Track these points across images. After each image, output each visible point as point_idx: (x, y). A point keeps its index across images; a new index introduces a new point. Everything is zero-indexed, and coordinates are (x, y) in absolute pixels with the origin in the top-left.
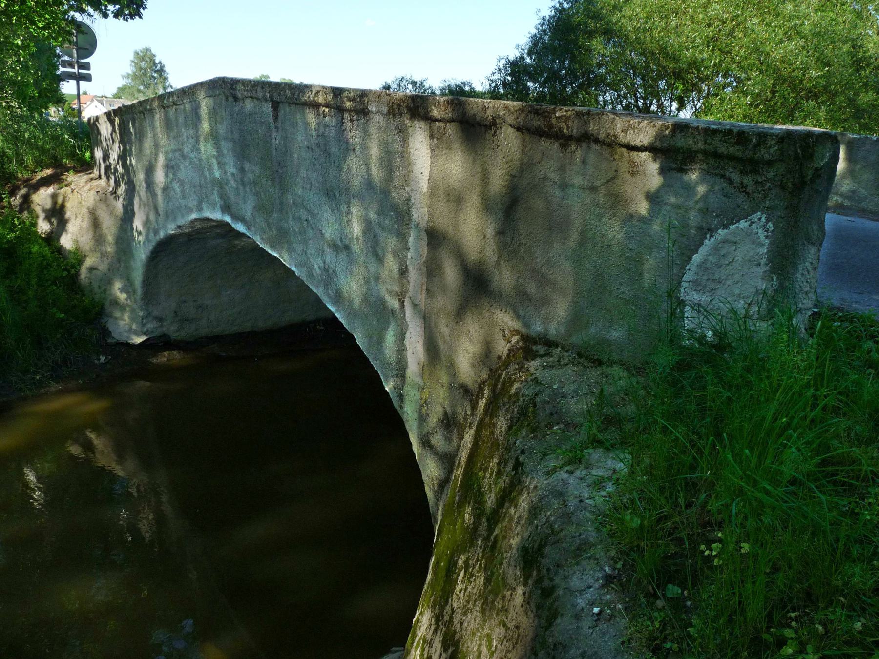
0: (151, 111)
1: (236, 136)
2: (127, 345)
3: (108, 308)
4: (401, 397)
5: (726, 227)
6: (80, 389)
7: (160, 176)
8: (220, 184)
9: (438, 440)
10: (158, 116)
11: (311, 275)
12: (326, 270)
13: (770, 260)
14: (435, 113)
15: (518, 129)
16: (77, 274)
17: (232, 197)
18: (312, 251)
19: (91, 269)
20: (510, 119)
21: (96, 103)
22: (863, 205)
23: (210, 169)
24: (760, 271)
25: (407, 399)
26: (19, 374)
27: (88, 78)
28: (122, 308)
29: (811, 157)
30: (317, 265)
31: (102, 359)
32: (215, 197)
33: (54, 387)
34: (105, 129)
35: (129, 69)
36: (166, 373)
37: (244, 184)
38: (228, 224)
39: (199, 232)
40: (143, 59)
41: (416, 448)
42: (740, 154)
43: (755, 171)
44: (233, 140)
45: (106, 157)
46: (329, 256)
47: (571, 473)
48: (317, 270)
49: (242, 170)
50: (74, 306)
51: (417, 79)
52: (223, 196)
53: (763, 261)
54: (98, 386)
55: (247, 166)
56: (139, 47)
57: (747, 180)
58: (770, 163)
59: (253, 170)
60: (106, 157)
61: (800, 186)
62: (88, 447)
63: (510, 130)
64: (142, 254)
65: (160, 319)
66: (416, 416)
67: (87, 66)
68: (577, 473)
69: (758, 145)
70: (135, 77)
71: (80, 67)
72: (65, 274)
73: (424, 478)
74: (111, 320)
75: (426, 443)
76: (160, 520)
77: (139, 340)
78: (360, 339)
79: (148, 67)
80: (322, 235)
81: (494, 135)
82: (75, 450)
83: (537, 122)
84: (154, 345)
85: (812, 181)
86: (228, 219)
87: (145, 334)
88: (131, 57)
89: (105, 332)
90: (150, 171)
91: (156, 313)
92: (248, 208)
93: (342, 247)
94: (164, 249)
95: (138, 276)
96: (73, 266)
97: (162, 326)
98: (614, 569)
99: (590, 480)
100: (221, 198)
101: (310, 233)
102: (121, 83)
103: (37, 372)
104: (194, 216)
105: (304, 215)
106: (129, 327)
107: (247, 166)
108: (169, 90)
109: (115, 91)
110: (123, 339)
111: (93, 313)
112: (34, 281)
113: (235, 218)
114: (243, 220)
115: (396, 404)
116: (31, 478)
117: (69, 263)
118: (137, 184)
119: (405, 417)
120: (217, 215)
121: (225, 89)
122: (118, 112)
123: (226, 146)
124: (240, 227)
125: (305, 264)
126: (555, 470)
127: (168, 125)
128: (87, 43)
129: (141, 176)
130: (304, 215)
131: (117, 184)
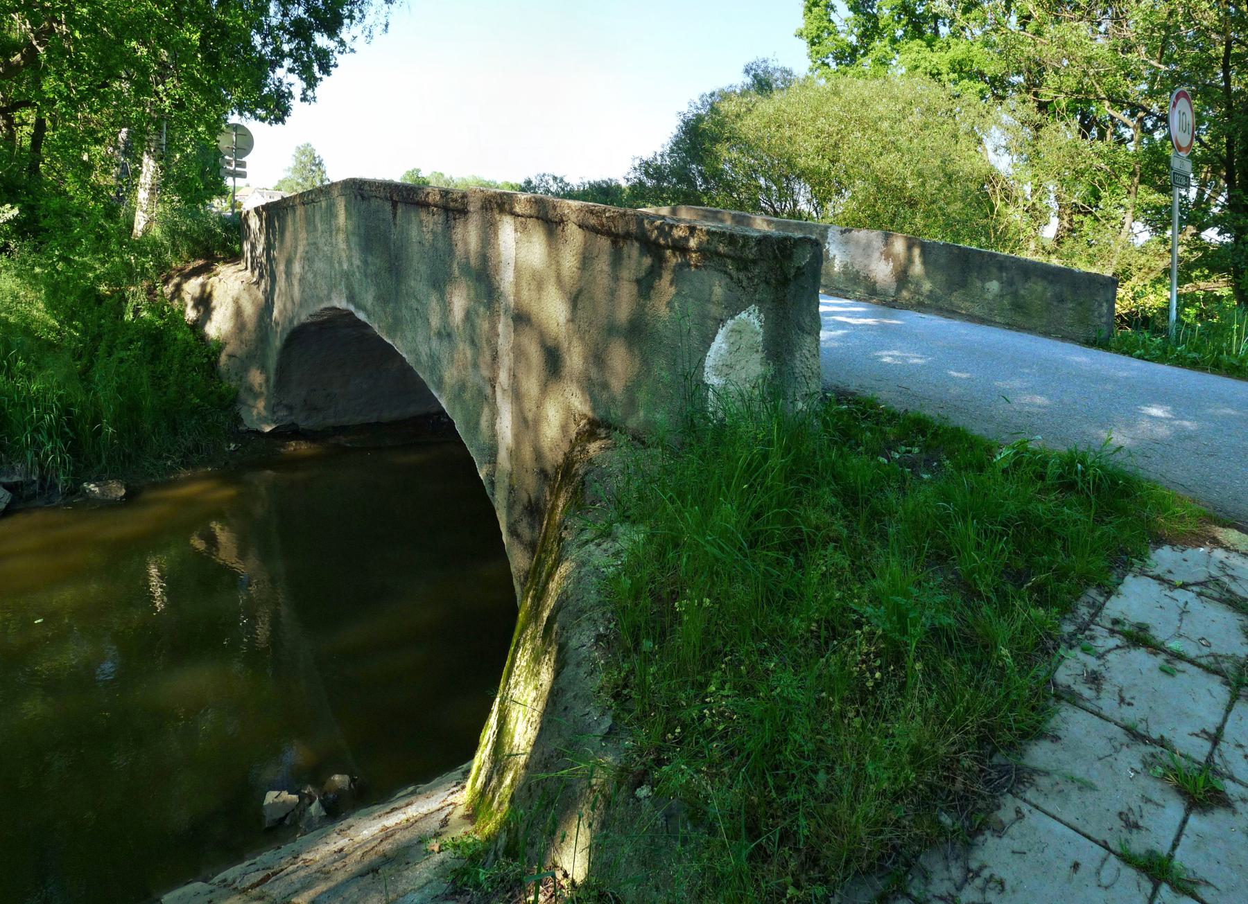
0: (293, 207)
1: (362, 231)
2: (259, 433)
3: (243, 395)
4: (492, 483)
5: (732, 317)
6: (208, 477)
7: (297, 268)
8: (347, 275)
9: (524, 530)
10: (300, 211)
11: (418, 361)
12: (431, 356)
13: (766, 348)
14: (518, 209)
15: (580, 226)
16: (217, 361)
17: (356, 286)
18: (420, 338)
19: (230, 356)
20: (573, 217)
21: (257, 194)
22: (940, 303)
23: (340, 263)
24: (758, 357)
25: (497, 485)
26: (152, 460)
27: (243, 175)
28: (257, 396)
29: (790, 257)
30: (424, 350)
31: (233, 446)
32: (343, 287)
33: (184, 473)
34: (254, 223)
35: (292, 163)
36: (294, 462)
37: (366, 276)
38: (352, 314)
39: (329, 321)
40: (303, 153)
41: (505, 538)
42: (731, 253)
43: (746, 269)
44: (359, 235)
45: (253, 248)
46: (435, 343)
47: (599, 545)
48: (424, 358)
49: (365, 262)
50: (211, 393)
51: (558, 175)
52: (350, 287)
53: (760, 349)
54: (229, 474)
55: (370, 259)
56: (301, 143)
57: (742, 275)
58: (754, 262)
59: (376, 262)
60: (253, 248)
61: (784, 282)
62: (211, 540)
63: (575, 227)
64: (277, 343)
65: (290, 408)
66: (505, 503)
67: (243, 165)
68: (604, 546)
69: (743, 246)
70: (295, 170)
71: (237, 165)
72: (205, 360)
73: (513, 570)
74: (245, 408)
75: (513, 532)
76: (275, 625)
77: (268, 429)
78: (459, 427)
79: (310, 162)
80: (429, 323)
81: (563, 230)
82: (198, 544)
83: (593, 221)
84: (286, 433)
85: (796, 276)
86: (352, 308)
87: (275, 422)
88: (293, 151)
89: (238, 420)
90: (289, 263)
91: (285, 402)
92: (369, 298)
93: (446, 334)
94: (299, 336)
95: (272, 362)
96: (214, 354)
97: (291, 414)
98: (607, 628)
99: (612, 550)
100: (347, 288)
101: (419, 322)
102: (282, 176)
103: (168, 458)
104: (323, 306)
105: (414, 304)
106: (259, 415)
107: (370, 259)
108: (326, 183)
109: (276, 183)
110: (254, 427)
111: (229, 403)
112: (176, 367)
113: (358, 307)
114: (364, 309)
115: (488, 491)
116: (154, 571)
117: (211, 350)
118: (278, 274)
119: (496, 505)
120: (341, 303)
121: (358, 190)
122: (267, 207)
123: (354, 240)
124: (361, 316)
125: (415, 352)
126: (587, 542)
127: (309, 221)
128: (245, 143)
129: (282, 267)
130: (414, 304)
131: (261, 276)
